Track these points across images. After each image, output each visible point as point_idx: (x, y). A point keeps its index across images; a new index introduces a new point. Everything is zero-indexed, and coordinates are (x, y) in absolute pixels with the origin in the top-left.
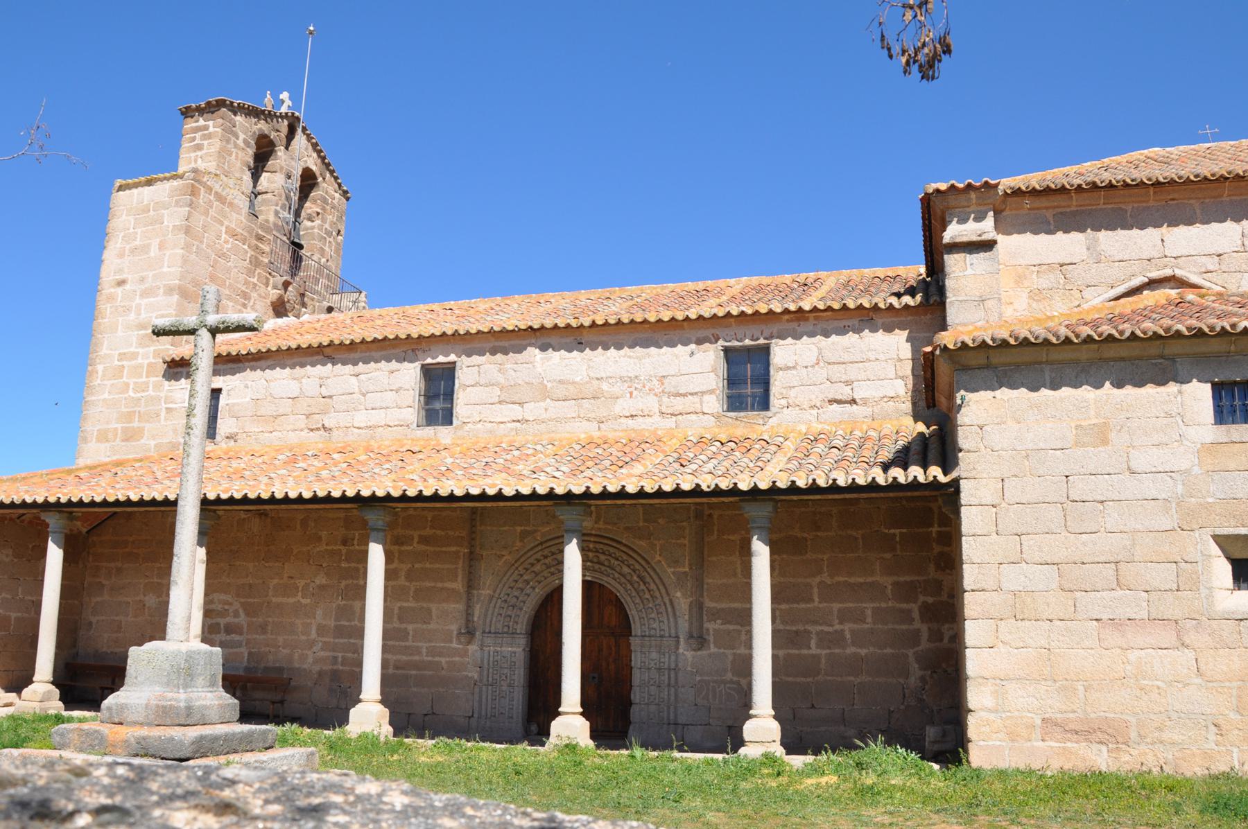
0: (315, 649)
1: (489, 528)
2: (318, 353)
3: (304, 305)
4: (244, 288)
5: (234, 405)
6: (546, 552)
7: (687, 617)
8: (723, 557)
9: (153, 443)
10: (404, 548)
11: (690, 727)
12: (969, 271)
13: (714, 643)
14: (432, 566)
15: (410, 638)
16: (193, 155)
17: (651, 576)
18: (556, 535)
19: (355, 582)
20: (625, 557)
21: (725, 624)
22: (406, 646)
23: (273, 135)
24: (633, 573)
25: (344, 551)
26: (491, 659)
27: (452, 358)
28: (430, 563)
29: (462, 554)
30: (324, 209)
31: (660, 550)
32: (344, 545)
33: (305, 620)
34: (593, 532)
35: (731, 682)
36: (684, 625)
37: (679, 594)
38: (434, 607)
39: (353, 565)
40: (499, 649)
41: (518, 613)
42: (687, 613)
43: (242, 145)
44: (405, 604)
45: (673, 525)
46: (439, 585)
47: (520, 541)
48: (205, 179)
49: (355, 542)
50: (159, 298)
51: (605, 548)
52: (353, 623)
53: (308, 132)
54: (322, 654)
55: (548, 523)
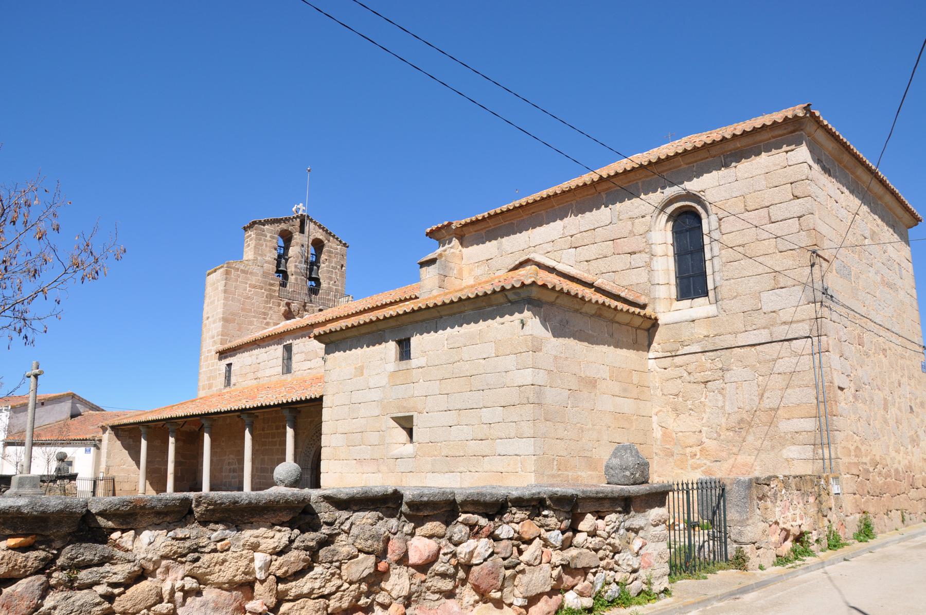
3: (306, 311)
4: (263, 311)
10: (279, 431)
12: (428, 276)
27: (291, 341)
30: (330, 256)
43: (269, 239)
44: (279, 457)
50: (217, 324)
54: (258, 480)
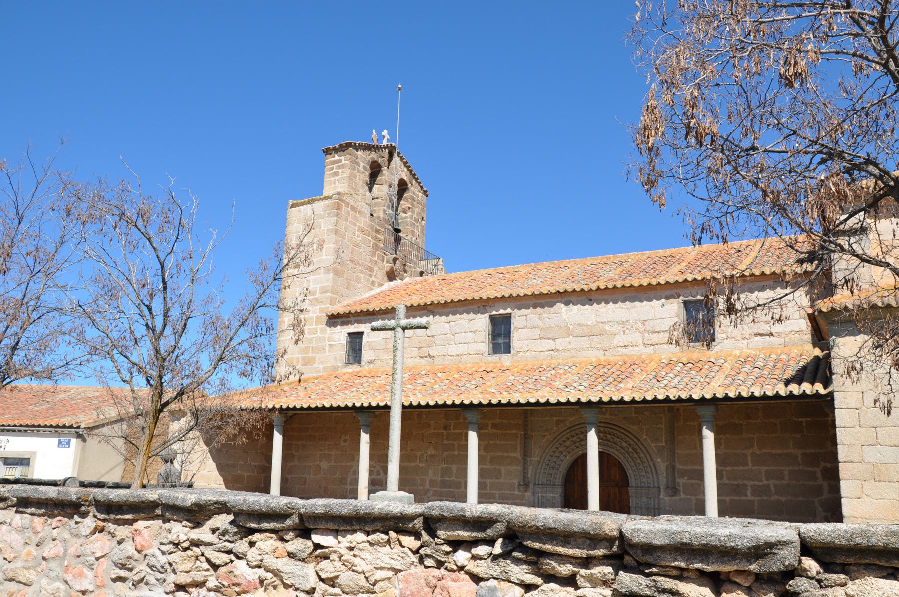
0: (428, 495)
1: (536, 418)
2: (423, 309)
3: (405, 271)
4: (369, 265)
5: (372, 342)
6: (573, 433)
7: (665, 475)
9: (321, 366)
13: (683, 492)
15: (488, 488)
16: (332, 179)
17: (641, 449)
18: (579, 422)
19: (452, 453)
20: (624, 436)
23: (380, 160)
25: (445, 434)
26: (540, 501)
27: (509, 311)
30: (412, 204)
32: (445, 430)
33: (422, 477)
34: (603, 421)
36: (663, 481)
37: (659, 460)
38: (503, 468)
39: (451, 442)
40: (545, 495)
41: (556, 472)
42: (665, 472)
46: (506, 454)
47: (556, 426)
48: (344, 198)
49: (452, 428)
50: (321, 275)
51: (611, 431)
52: (452, 479)
53: (401, 155)
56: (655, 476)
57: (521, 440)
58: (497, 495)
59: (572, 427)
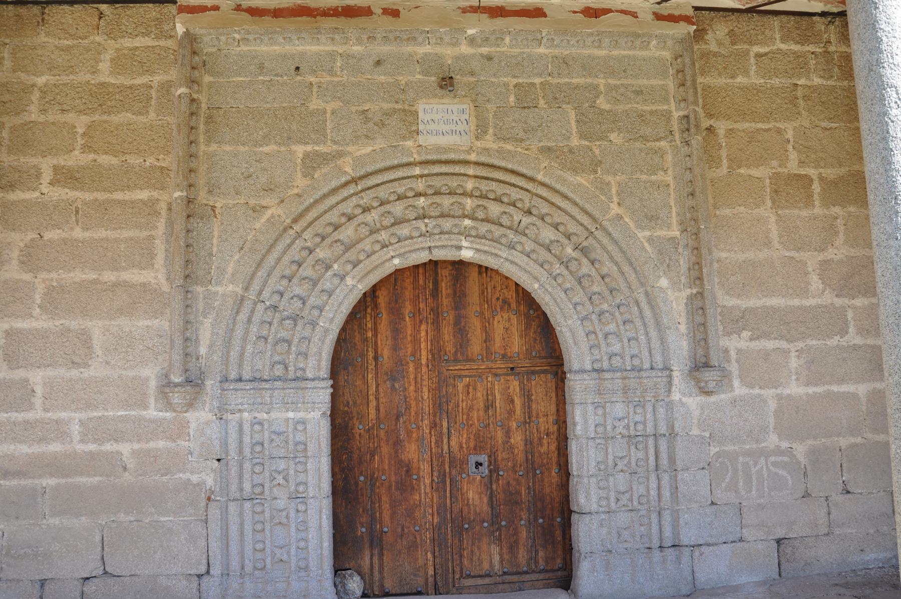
1: (228, 148)
6: (366, 199)
7: (683, 328)
8: (742, 209)
11: (703, 549)
13: (742, 378)
14: (87, 234)
15: (38, 401)
17: (604, 248)
18: (388, 163)
20: (545, 208)
21: (758, 338)
22: (27, 422)
24: (566, 241)
26: (247, 440)
28: (86, 229)
29: (163, 206)
31: (618, 194)
34: (473, 157)
35: (779, 452)
37: (664, 282)
38: (96, 328)
41: (306, 333)
42: (683, 320)
45: (638, 145)
46: (109, 277)
47: (305, 176)
51: (500, 189)
55: (367, 137)
56: (653, 334)
57: (170, 223)
58: (75, 428)
59: (362, 178)
